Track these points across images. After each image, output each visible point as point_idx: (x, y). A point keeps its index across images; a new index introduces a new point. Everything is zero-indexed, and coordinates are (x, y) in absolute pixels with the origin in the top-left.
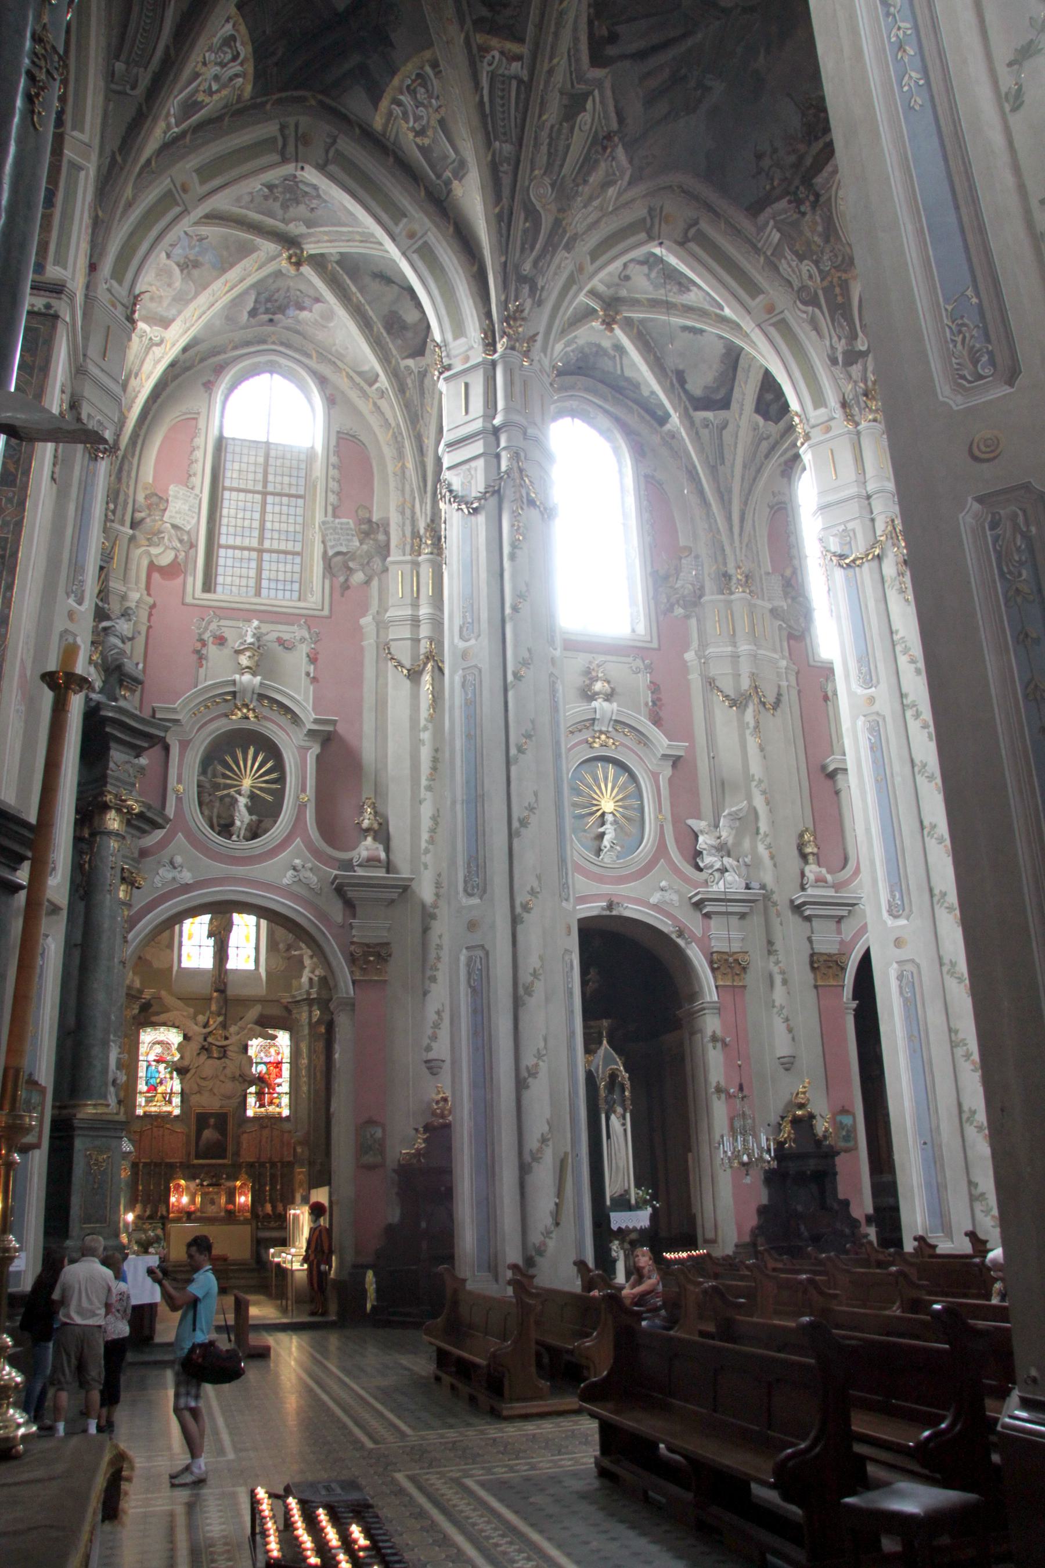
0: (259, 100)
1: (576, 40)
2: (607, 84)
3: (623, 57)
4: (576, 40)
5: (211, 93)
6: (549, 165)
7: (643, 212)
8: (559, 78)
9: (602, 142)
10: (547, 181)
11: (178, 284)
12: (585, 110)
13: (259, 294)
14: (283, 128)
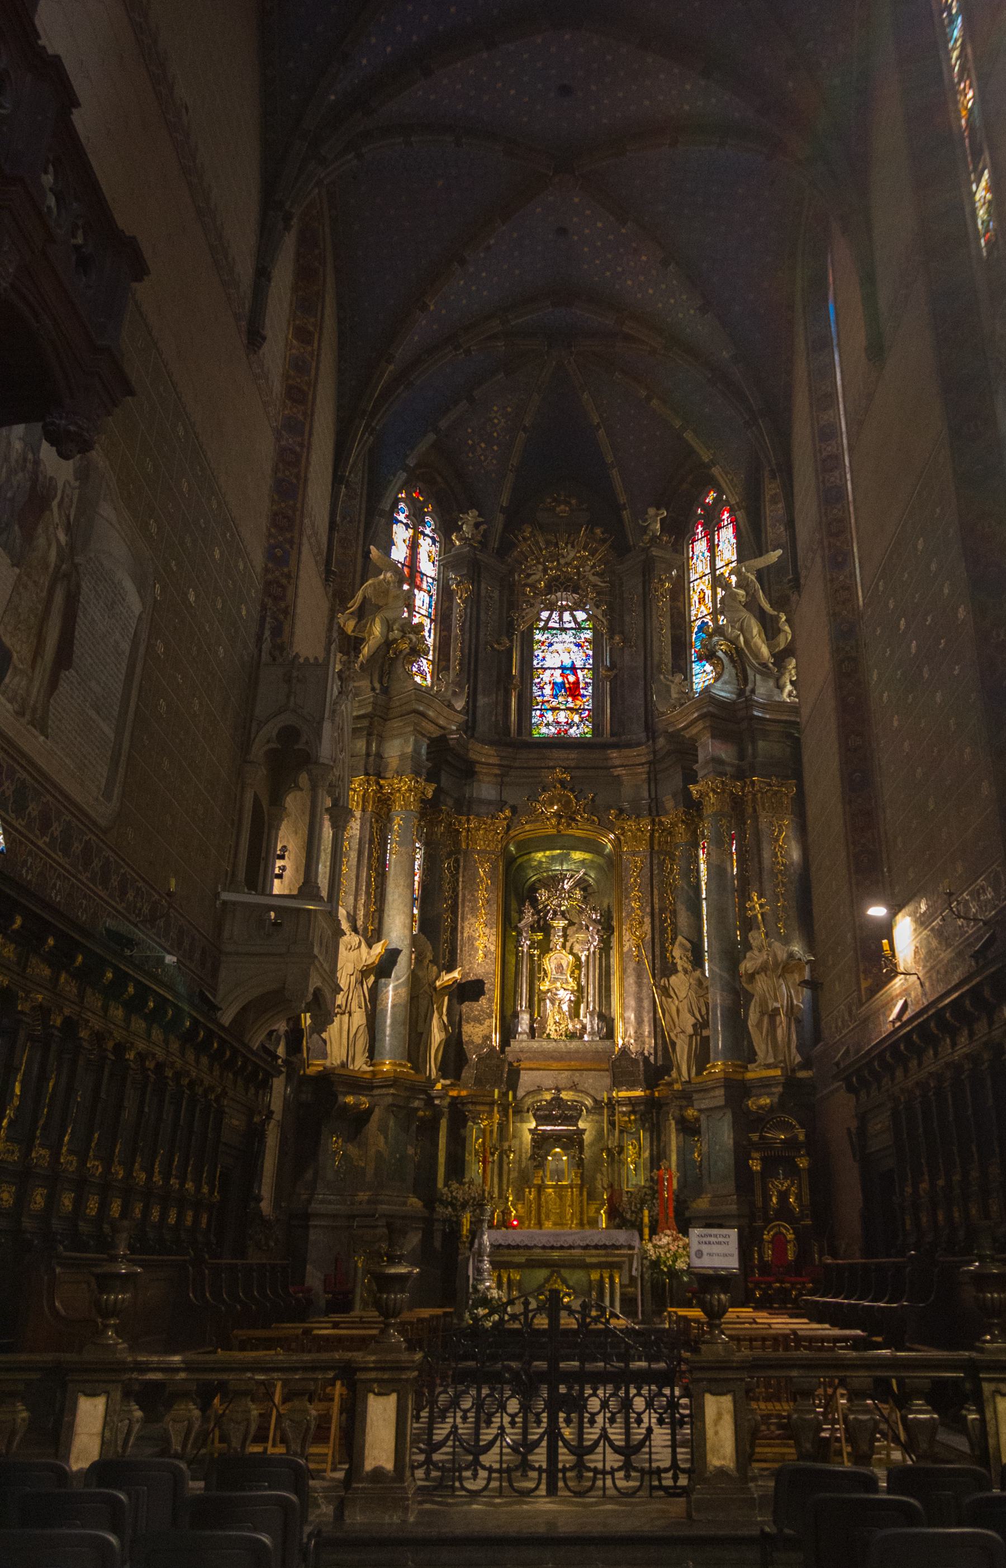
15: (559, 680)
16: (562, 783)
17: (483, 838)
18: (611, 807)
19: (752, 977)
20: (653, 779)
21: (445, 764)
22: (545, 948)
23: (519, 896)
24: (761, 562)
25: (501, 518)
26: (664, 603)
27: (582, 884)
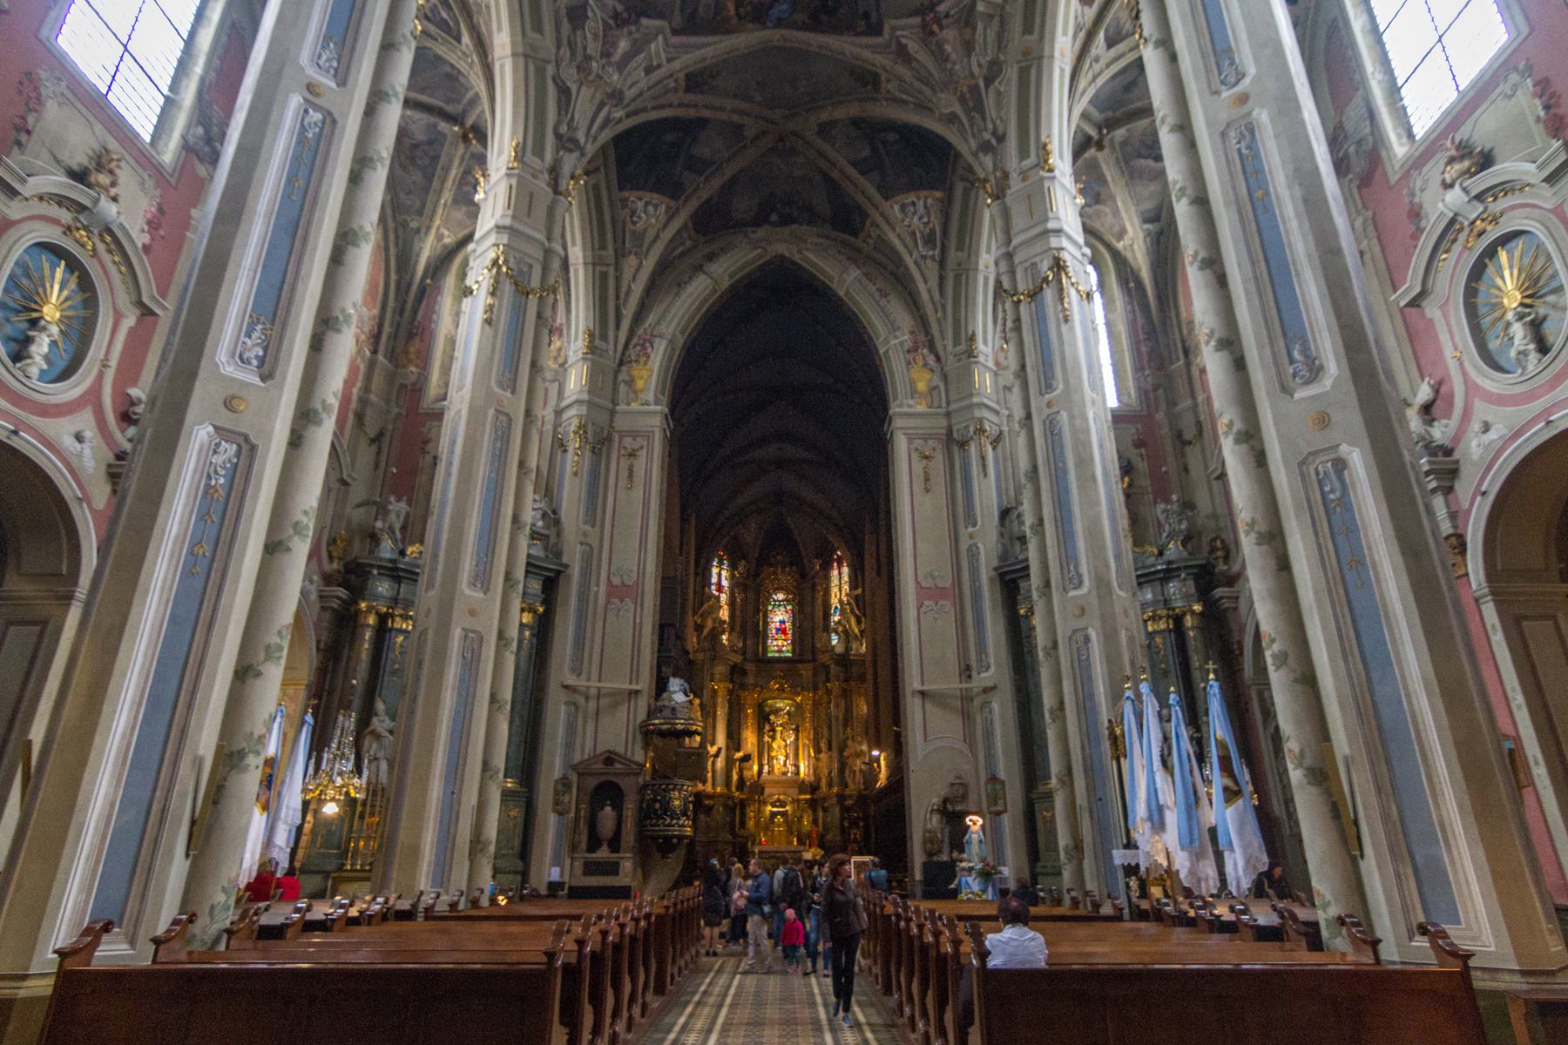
1: (867, 46)
2: (894, 22)
4: (867, 46)
6: (933, 90)
8: (888, 64)
9: (927, 33)
11: (1107, 210)
13: (1140, 156)
14: (963, 180)
17: (751, 698)
20: (815, 675)
21: (736, 672)
22: (773, 738)
23: (764, 719)
26: (819, 601)
27: (789, 713)
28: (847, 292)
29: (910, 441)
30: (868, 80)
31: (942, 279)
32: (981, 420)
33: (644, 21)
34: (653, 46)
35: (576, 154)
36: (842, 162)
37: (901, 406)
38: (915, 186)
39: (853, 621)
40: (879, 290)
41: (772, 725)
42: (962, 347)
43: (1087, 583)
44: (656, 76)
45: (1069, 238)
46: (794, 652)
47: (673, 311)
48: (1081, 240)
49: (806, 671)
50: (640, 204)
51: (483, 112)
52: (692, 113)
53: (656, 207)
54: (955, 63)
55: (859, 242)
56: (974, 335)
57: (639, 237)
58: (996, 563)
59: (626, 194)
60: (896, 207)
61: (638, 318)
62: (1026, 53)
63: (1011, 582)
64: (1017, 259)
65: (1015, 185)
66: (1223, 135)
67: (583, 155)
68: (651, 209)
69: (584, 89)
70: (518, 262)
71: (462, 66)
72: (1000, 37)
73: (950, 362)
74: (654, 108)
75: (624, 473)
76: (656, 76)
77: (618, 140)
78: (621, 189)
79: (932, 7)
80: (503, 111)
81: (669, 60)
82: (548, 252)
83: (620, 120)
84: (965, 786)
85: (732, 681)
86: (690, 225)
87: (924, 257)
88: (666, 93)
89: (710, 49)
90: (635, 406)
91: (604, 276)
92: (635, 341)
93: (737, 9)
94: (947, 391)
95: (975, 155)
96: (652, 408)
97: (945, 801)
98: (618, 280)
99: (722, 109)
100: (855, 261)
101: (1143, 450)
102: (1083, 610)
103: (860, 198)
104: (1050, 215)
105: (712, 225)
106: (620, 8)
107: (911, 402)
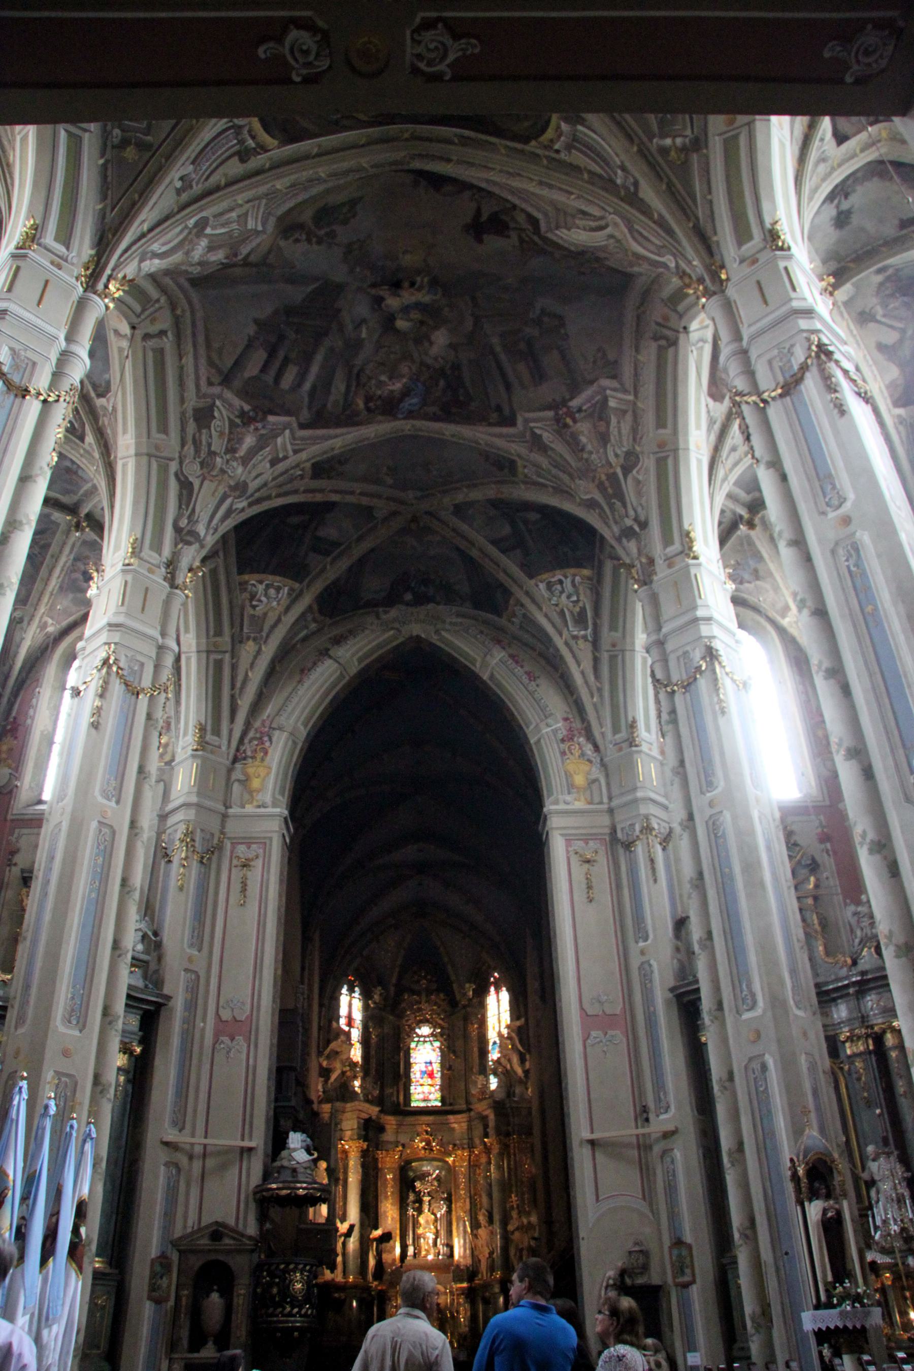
0: (596, 563)
3: (510, 399)
4: (500, 436)
5: (578, 601)
6: (572, 477)
7: (653, 346)
9: (561, 427)
10: (578, 481)
11: (767, 586)
12: (540, 436)
15: (424, 1069)
16: (427, 1132)
18: (449, 1143)
19: (513, 1233)
20: (470, 1129)
23: (407, 1184)
24: (518, 1023)
25: (392, 989)
27: (438, 1178)
28: (492, 677)
29: (568, 842)
30: (505, 466)
31: (596, 661)
32: (648, 819)
33: (271, 419)
34: (279, 440)
35: (196, 546)
36: (481, 540)
37: (556, 802)
38: (562, 563)
39: (515, 1059)
40: (528, 673)
41: (418, 1194)
42: (623, 735)
43: (761, 1003)
44: (281, 467)
45: (720, 625)
46: (443, 1100)
47: (295, 700)
48: (733, 625)
49: (458, 1124)
50: (261, 588)
51: (100, 501)
52: (319, 497)
53: (278, 589)
54: (591, 453)
55: (503, 622)
56: (634, 721)
57: (258, 622)
58: (671, 983)
59: (246, 577)
60: (542, 586)
61: (256, 707)
62: (661, 445)
63: (687, 1006)
64: (669, 646)
65: (662, 572)
66: (833, 552)
67: (202, 546)
68: (272, 592)
69: (206, 483)
70: (132, 660)
71: (82, 462)
72: (634, 430)
73: (611, 754)
74: (279, 496)
75: (236, 887)
76: (281, 467)
77: (237, 528)
78: (241, 572)
79: (564, 402)
80: (123, 507)
81: (296, 452)
82: (161, 648)
83: (243, 510)
84: (645, 1253)
85: (366, 1139)
86: (315, 607)
87: (575, 638)
88: (291, 480)
89: (339, 440)
90: (249, 809)
91: (219, 664)
92: (251, 734)
93: (366, 403)
94: (608, 784)
95: (619, 540)
96: (270, 810)
97: (623, 1273)
98: (234, 667)
99: (352, 493)
100: (499, 642)
101: (828, 845)
102: (759, 1035)
103: (501, 576)
104: (699, 602)
105: (339, 606)
106: (247, 408)
107: (568, 798)
